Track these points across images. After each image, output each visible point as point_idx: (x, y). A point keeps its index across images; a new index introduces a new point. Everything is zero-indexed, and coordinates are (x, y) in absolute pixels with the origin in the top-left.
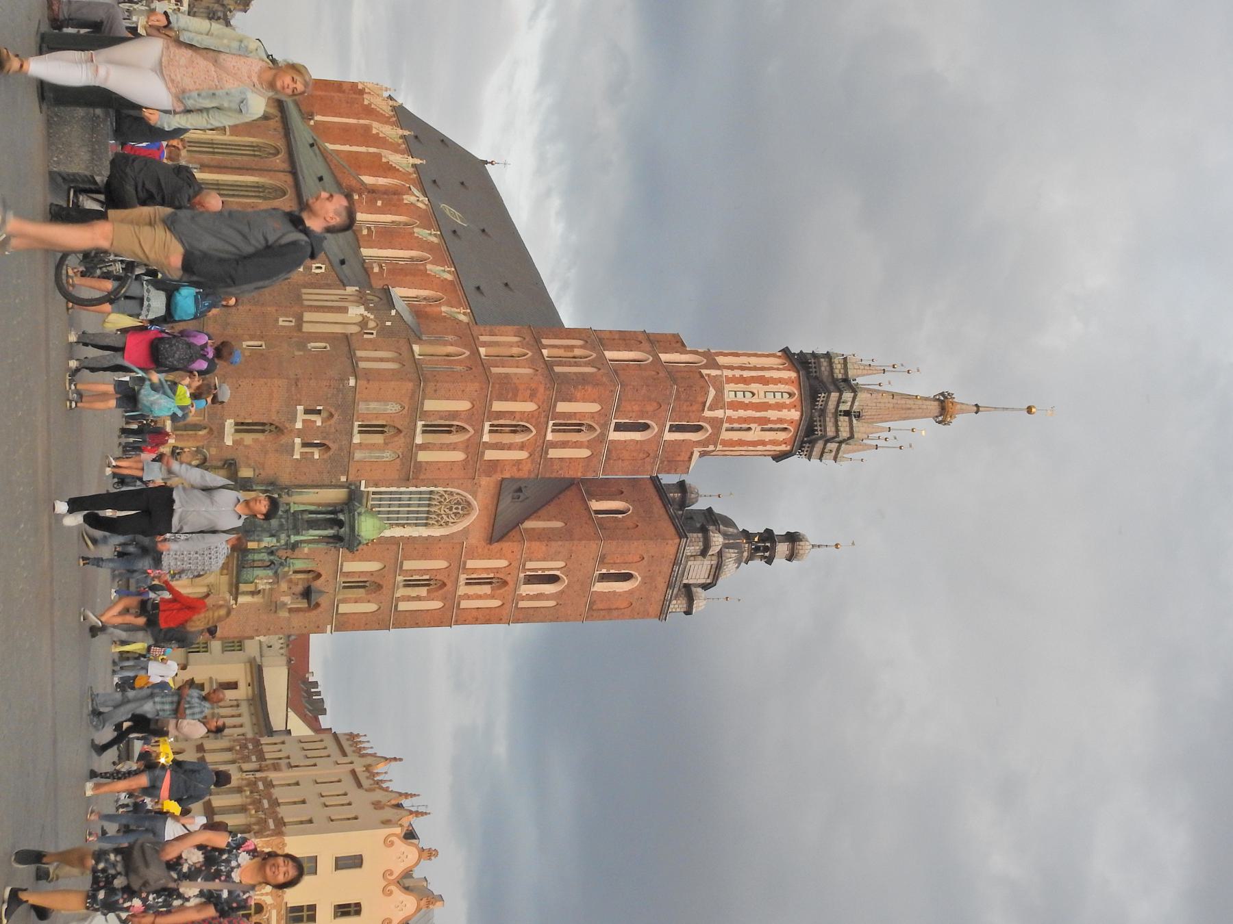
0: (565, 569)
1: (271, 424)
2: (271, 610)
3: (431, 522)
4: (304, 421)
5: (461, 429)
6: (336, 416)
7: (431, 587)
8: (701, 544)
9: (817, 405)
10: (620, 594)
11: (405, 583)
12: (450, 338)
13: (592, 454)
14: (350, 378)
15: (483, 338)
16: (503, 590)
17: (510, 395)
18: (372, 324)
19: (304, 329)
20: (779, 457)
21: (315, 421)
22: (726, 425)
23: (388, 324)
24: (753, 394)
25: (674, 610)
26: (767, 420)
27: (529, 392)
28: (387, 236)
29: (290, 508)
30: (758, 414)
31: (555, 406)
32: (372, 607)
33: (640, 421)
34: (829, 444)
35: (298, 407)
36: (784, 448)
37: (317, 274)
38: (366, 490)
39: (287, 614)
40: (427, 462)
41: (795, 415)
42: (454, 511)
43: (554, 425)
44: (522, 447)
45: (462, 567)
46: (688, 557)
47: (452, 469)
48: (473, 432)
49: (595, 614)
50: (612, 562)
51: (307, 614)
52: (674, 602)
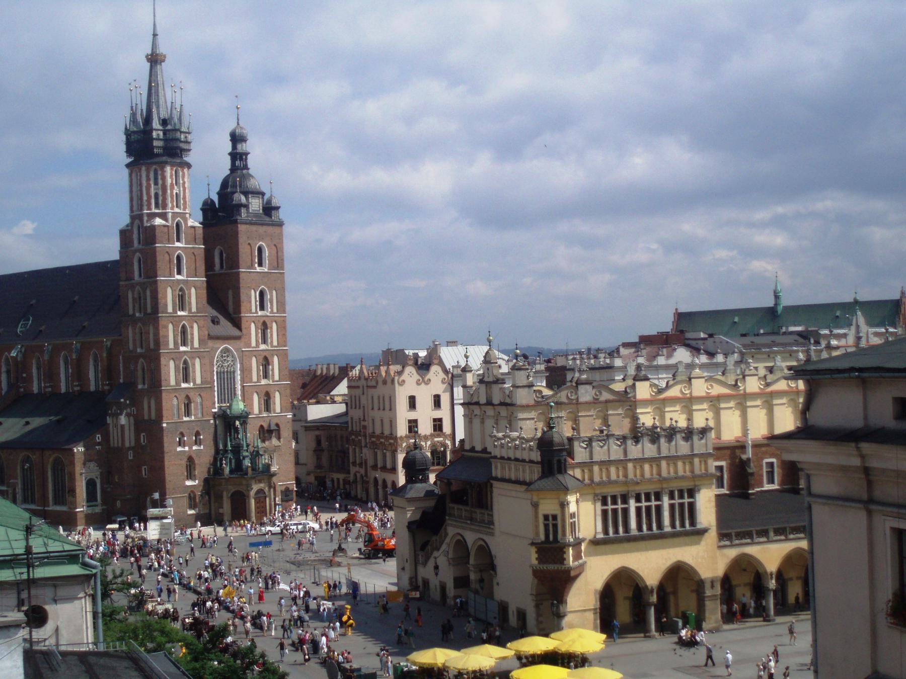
3: (232, 369)
4: (184, 446)
5: (185, 362)
6: (181, 430)
10: (269, 252)
12: (132, 368)
15: (131, 346)
16: (268, 323)
22: (177, 210)
23: (128, 402)
26: (172, 184)
28: (51, 375)
31: (171, 313)
32: (277, 395)
34: (182, 140)
40: (201, 378)
41: (168, 169)
43: (179, 310)
44: (192, 327)
46: (248, 212)
48: (185, 357)
49: (280, 266)
51: (282, 429)
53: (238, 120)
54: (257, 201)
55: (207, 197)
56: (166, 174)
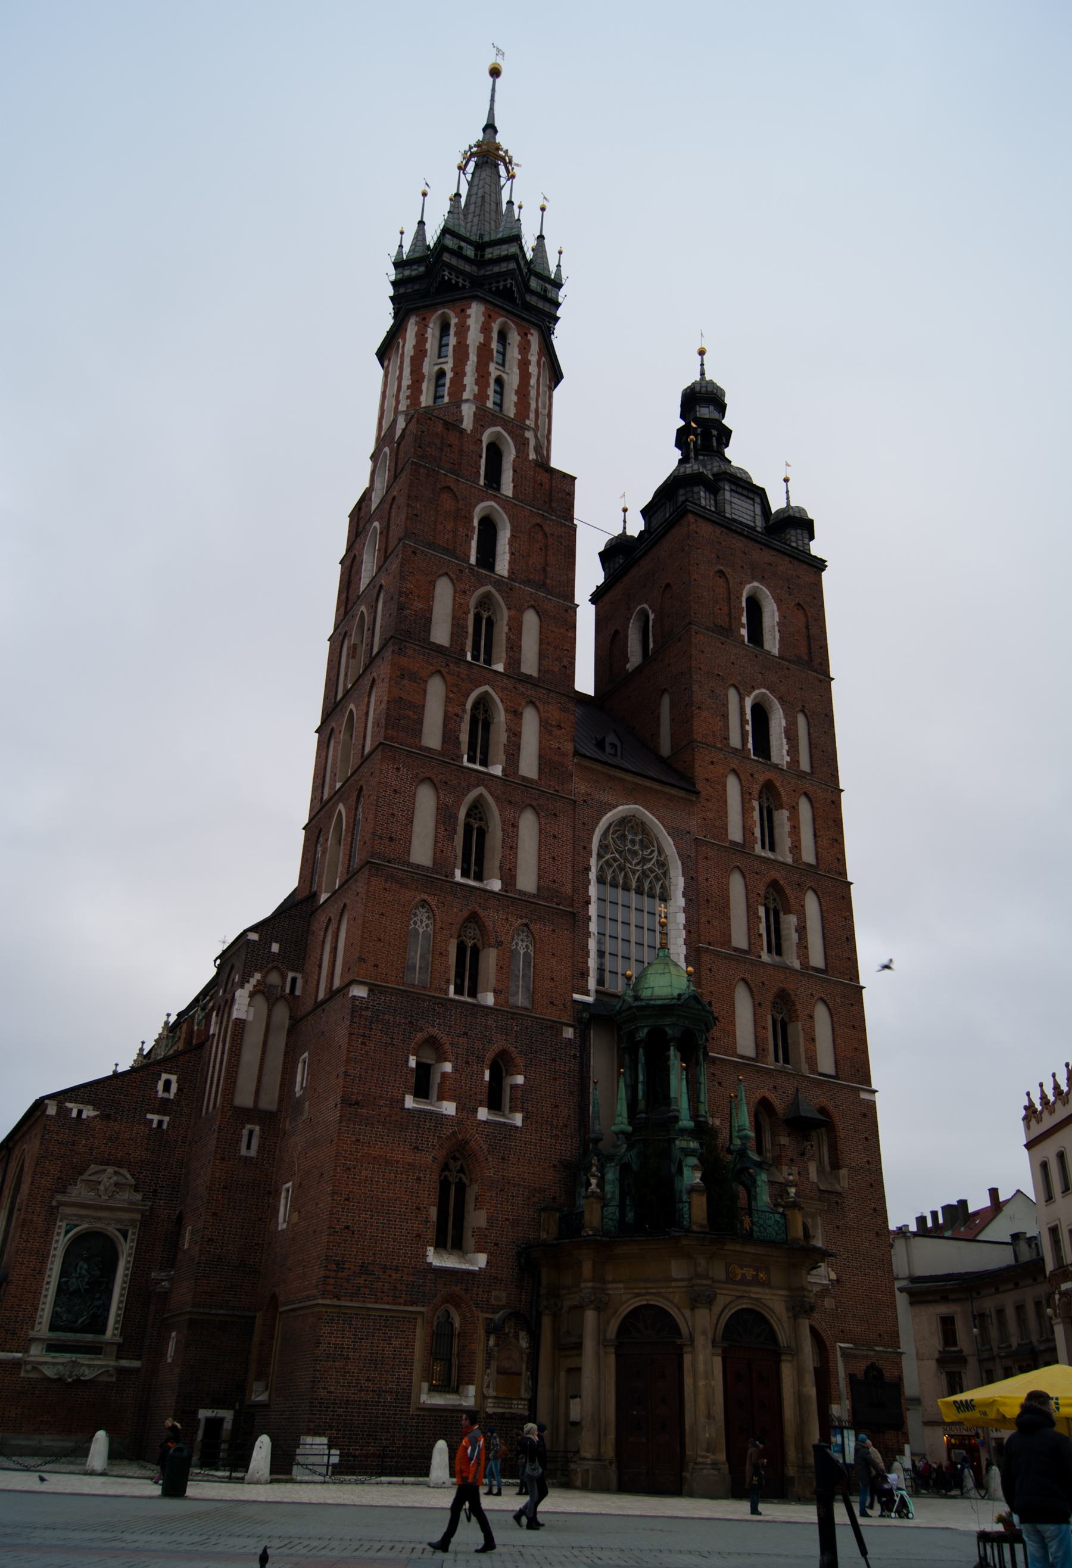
1: (446, 1167)
2: (837, 1203)
4: (441, 1098)
5: (477, 809)
6: (434, 1031)
7: (780, 908)
8: (696, 489)
9: (464, 286)
10: (783, 617)
13: (533, 607)
14: (350, 995)
18: (274, 978)
19: (274, 1107)
20: (556, 376)
21: (444, 1075)
23: (275, 948)
24: (441, 374)
27: (406, 682)
29: (623, 1132)
30: (473, 358)
31: (439, 649)
32: (821, 1015)
33: (476, 523)
36: (534, 340)
37: (179, 1089)
38: (592, 993)
39: (844, 1172)
40: (540, 877)
41: (476, 313)
42: (637, 847)
44: (516, 715)
45: (742, 849)
47: (555, 836)
48: (481, 790)
50: (727, 620)
51: (842, 1134)
52: (794, 544)
53: (702, 374)
54: (751, 507)
55: (621, 532)
56: (471, 322)
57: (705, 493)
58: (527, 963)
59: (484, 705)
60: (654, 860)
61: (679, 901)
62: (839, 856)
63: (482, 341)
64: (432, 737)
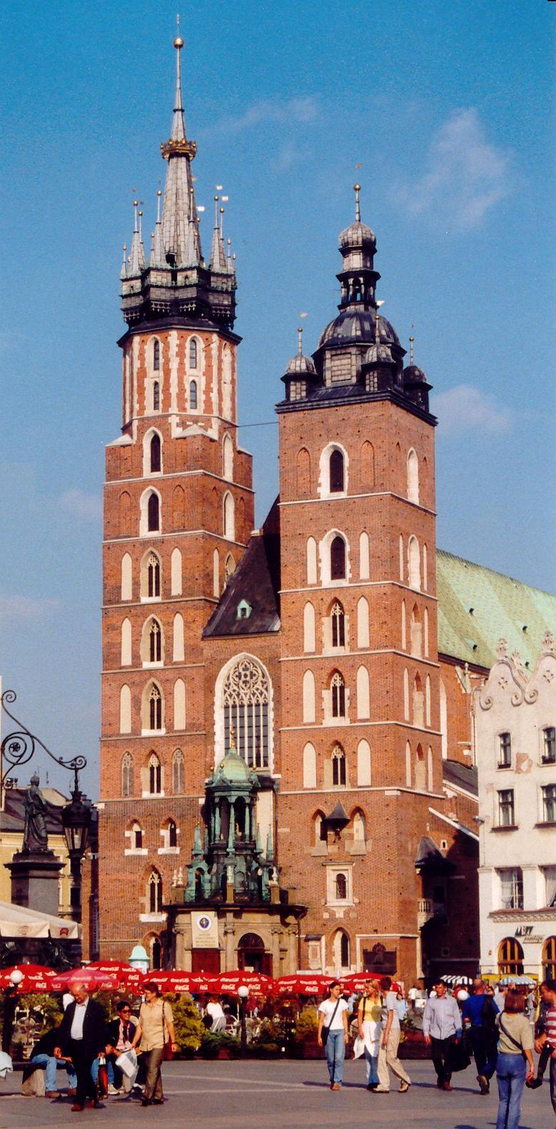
0: (316, 536)
6: (136, 817)
9: (136, 317)
10: (352, 460)
11: (339, 715)
17: (114, 650)
22: (150, 412)
25: (376, 385)
34: (179, 284)
35: (126, 854)
39: (370, 842)
40: (186, 718)
42: (248, 678)
43: (151, 595)
44: (170, 624)
48: (153, 680)
54: (349, 360)
57: (296, 385)
58: (182, 769)
59: (157, 624)
60: (259, 683)
61: (271, 705)
62: (386, 634)
63: (139, 366)
64: (126, 660)
